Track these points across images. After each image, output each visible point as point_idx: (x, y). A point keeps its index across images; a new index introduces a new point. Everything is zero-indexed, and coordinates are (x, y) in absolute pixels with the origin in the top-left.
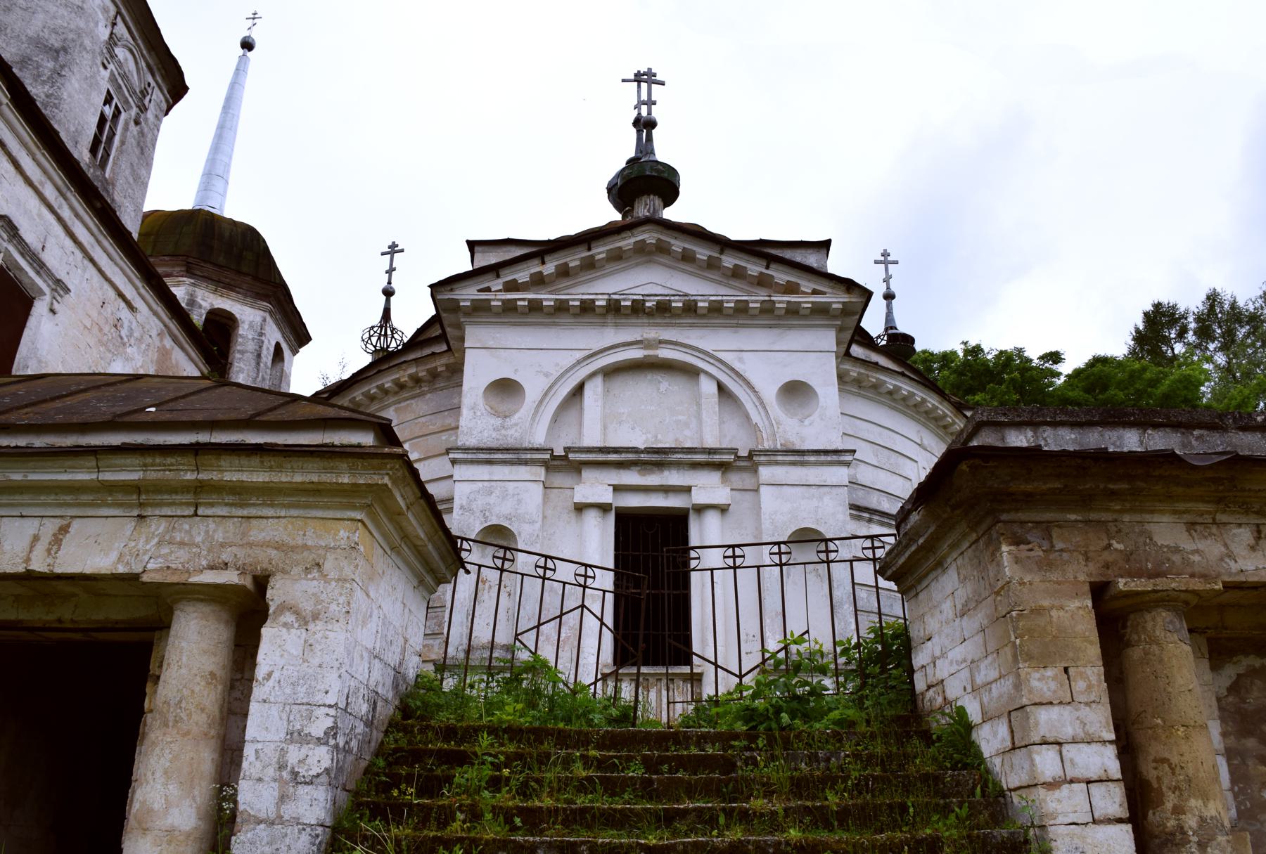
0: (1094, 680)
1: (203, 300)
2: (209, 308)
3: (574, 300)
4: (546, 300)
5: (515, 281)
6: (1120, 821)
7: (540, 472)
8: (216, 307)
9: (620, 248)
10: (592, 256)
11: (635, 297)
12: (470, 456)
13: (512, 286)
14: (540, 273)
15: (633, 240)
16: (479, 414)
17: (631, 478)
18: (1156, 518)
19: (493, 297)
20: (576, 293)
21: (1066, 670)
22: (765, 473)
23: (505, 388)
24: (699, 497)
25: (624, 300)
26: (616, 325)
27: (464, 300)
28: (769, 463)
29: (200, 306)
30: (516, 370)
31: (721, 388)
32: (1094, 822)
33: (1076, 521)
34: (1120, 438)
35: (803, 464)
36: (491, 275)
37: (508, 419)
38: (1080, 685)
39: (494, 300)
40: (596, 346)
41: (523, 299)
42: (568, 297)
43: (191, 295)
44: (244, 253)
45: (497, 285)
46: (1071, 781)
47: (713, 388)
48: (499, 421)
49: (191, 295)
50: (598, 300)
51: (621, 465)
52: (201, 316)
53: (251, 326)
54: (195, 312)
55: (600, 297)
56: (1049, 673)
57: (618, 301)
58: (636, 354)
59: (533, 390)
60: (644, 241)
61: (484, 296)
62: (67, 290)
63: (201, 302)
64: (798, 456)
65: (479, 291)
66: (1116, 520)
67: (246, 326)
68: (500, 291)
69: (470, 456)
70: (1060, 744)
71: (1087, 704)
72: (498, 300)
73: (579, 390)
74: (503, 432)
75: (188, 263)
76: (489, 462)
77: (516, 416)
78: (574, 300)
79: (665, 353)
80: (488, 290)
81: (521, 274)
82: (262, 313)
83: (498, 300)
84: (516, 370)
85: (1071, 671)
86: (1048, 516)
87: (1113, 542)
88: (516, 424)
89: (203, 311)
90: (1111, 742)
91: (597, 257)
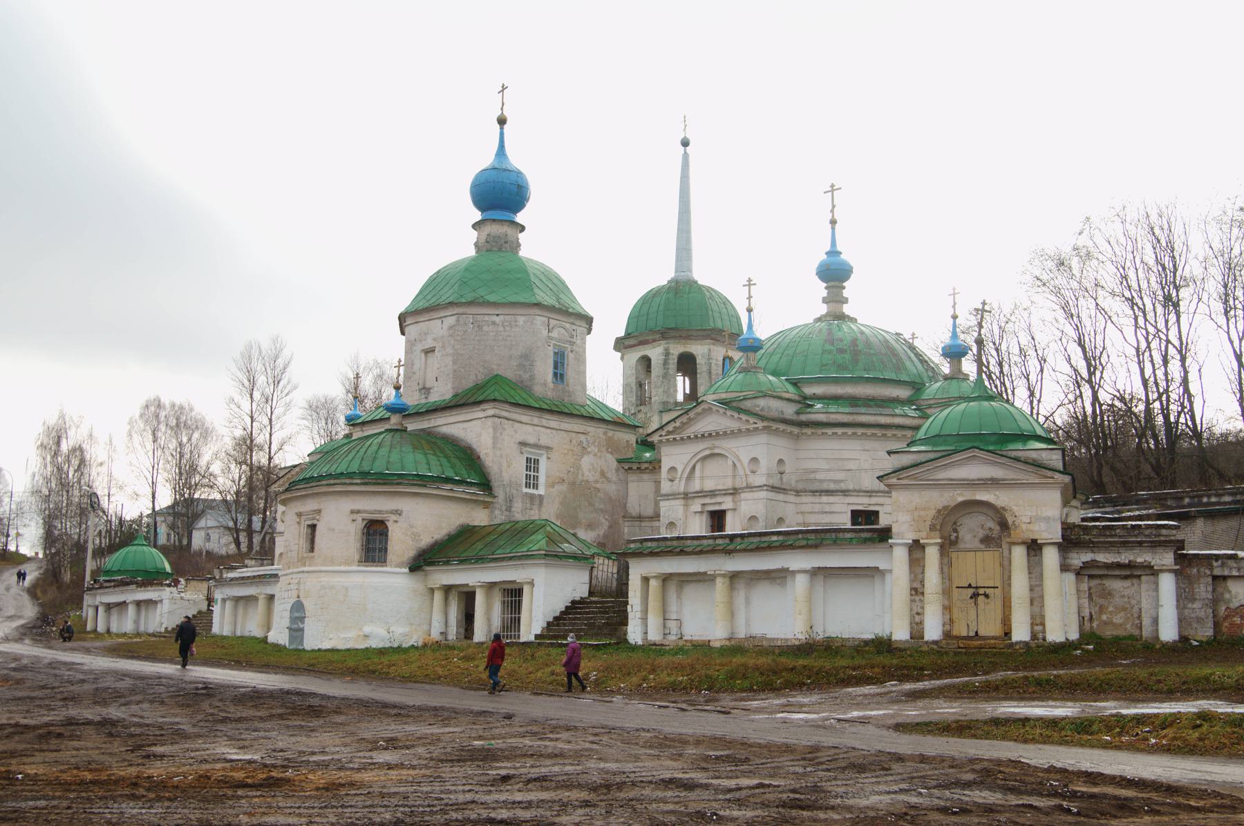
7: (682, 502)
13: (669, 433)
17: (707, 500)
20: (690, 431)
22: (743, 495)
23: (673, 469)
24: (723, 507)
28: (743, 492)
29: (673, 354)
31: (734, 464)
35: (753, 491)
45: (664, 433)
47: (731, 463)
51: (704, 496)
53: (703, 357)
58: (708, 452)
59: (680, 470)
62: (551, 448)
64: (750, 488)
67: (700, 357)
73: (694, 467)
76: (668, 499)
79: (716, 451)
80: (661, 436)
82: (708, 346)
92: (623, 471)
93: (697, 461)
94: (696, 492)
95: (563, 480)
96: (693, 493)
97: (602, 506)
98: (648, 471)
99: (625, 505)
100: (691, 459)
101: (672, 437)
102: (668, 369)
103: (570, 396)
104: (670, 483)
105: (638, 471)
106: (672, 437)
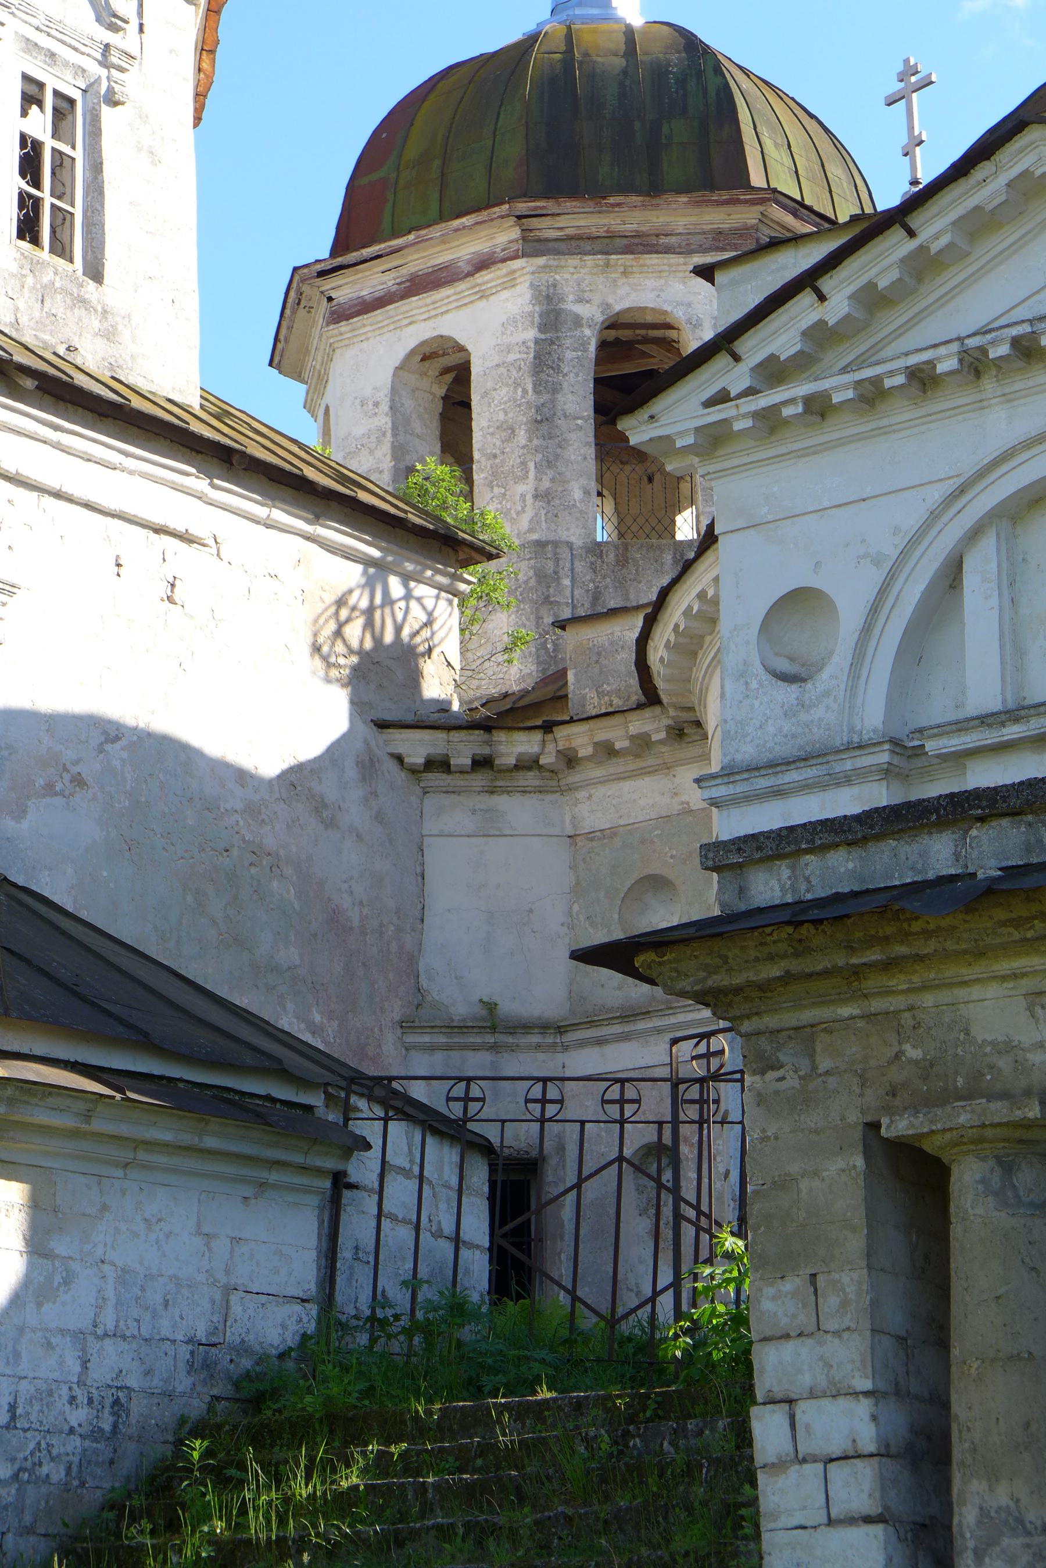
0: (851, 1290)
1: (580, 300)
2: (600, 318)
3: (891, 373)
4: (837, 388)
5: (773, 358)
6: (868, 1520)
8: (618, 308)
9: (977, 209)
10: (923, 248)
11: (1015, 331)
12: (739, 788)
14: (821, 323)
15: (1003, 179)
16: (754, 685)
18: (975, 992)
19: (733, 412)
21: (814, 1276)
25: (993, 343)
26: (1008, 399)
27: (681, 434)
29: (578, 321)
30: (818, 564)
32: (831, 1522)
33: (852, 1018)
34: (923, 855)
36: (722, 360)
37: (809, 685)
38: (830, 1302)
39: (736, 418)
40: (968, 464)
41: (791, 401)
42: (878, 370)
43: (548, 298)
44: (665, 129)
46: (804, 1461)
48: (792, 691)
49: (548, 298)
50: (939, 359)
52: (583, 345)
54: (568, 342)
55: (942, 351)
56: (788, 1286)
57: (983, 350)
60: (1025, 174)
61: (717, 414)
63: (579, 309)
65: (709, 403)
66: (911, 1008)
68: (750, 392)
69: (739, 788)
70: (790, 1402)
71: (837, 1333)
72: (744, 416)
74: (804, 717)
75: (519, 217)
77: (825, 675)
78: (891, 373)
80: (722, 398)
81: (783, 339)
83: (744, 416)
84: (818, 564)
85: (821, 1280)
86: (808, 1016)
87: (907, 1047)
88: (826, 694)
89: (587, 332)
90: (867, 1394)
91: (935, 247)
92: (400, 776)
93: (975, 534)
94: (984, 720)
95: (79, 781)
96: (961, 726)
97: (290, 955)
98: (530, 779)
99: (412, 960)
100: (934, 515)
101: (803, 389)
102: (555, 390)
103: (109, 335)
104: (788, 693)
105: (479, 780)
106: (803, 389)
